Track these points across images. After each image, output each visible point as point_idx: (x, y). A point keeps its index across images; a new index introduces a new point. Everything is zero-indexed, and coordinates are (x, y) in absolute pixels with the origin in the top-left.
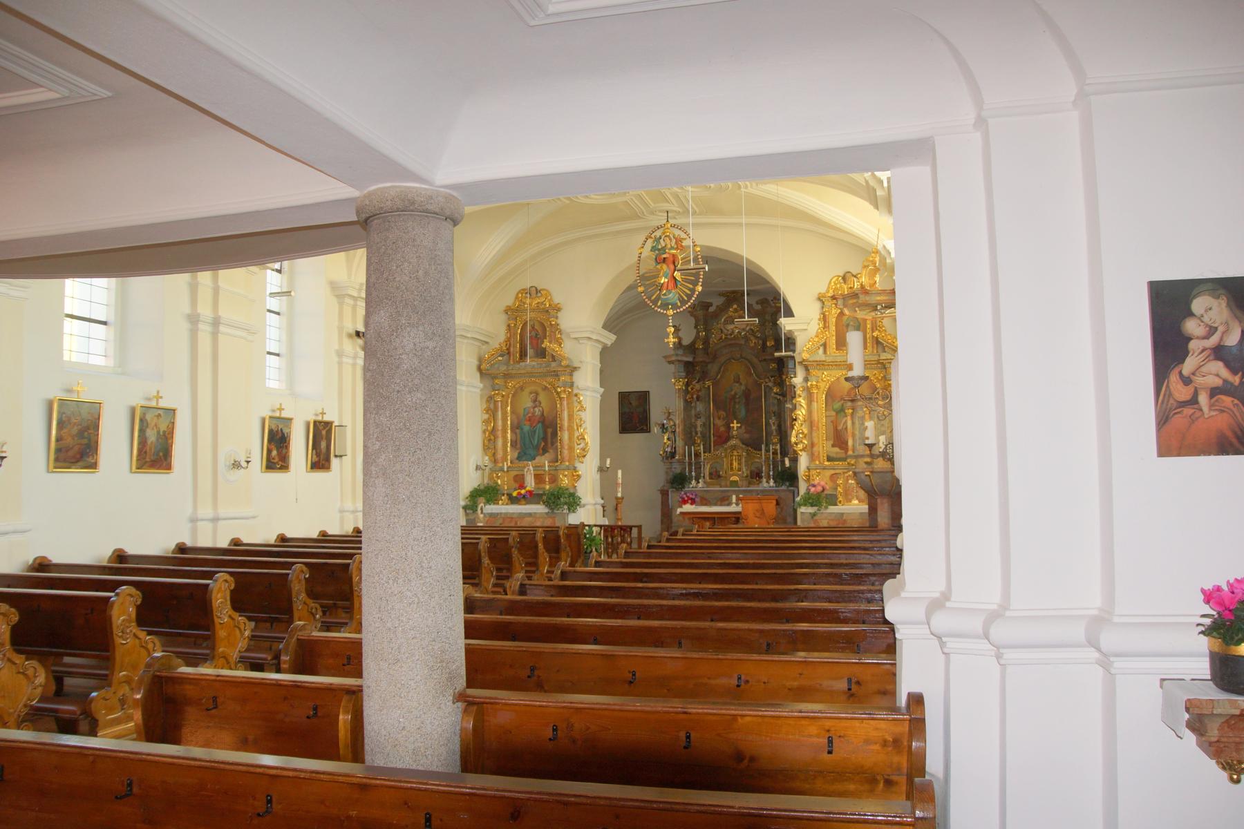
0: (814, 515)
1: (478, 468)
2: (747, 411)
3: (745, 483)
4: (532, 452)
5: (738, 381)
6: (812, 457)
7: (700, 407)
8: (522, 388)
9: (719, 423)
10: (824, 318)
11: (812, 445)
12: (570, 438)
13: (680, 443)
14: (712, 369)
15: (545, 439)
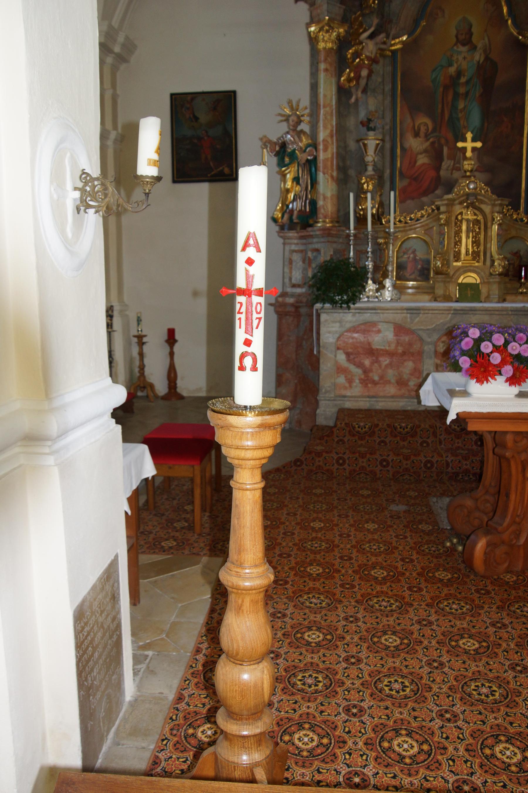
2: (486, 114)
3: (495, 290)
9: (415, 144)
13: (326, 187)
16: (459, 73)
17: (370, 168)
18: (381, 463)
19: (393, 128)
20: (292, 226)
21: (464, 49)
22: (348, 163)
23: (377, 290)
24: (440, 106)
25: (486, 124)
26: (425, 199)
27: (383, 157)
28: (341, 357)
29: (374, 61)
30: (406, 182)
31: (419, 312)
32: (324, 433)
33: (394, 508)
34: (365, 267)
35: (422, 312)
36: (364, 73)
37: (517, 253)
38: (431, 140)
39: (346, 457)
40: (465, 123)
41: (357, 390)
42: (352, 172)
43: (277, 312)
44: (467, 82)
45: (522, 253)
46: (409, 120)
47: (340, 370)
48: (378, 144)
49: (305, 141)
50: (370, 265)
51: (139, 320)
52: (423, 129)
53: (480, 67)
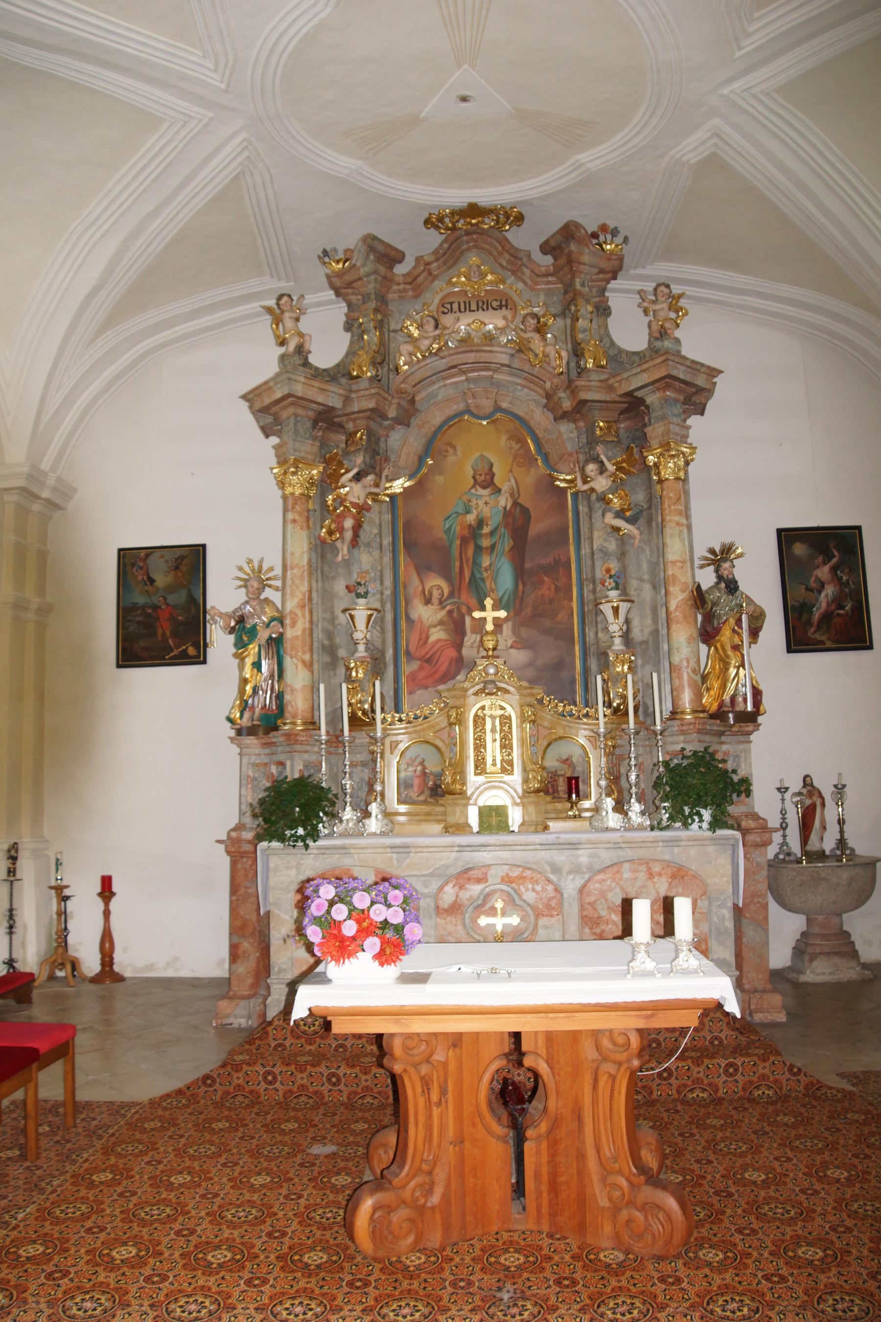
2: (520, 573)
5: (487, 481)
14: (403, 443)
16: (481, 523)
17: (361, 648)
18: (329, 1080)
20: (251, 731)
21: (486, 492)
22: (337, 640)
23: (359, 821)
24: (457, 564)
25: (521, 587)
26: (441, 687)
27: (383, 631)
30: (415, 665)
31: (407, 850)
33: (318, 1150)
34: (343, 788)
35: (413, 850)
36: (349, 523)
37: (567, 759)
38: (448, 608)
39: (276, 1070)
40: (493, 586)
42: (342, 653)
43: (228, 852)
44: (492, 533)
45: (574, 760)
46: (416, 582)
48: (371, 615)
51: (58, 864)
52: (436, 594)
53: (507, 514)
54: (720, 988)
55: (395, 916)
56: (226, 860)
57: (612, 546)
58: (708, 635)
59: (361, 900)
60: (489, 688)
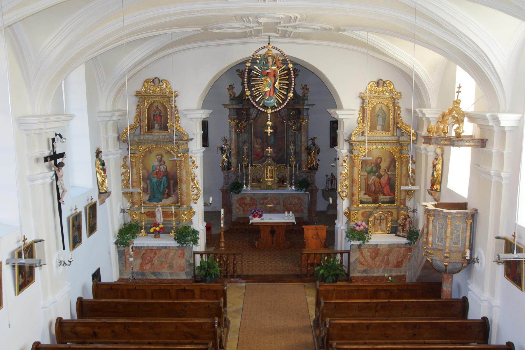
0: (359, 246)
1: (123, 211)
3: (276, 187)
4: (160, 197)
6: (352, 202)
7: (245, 136)
8: (150, 152)
9: (257, 146)
10: (363, 110)
11: (353, 195)
12: (187, 187)
13: (234, 160)
15: (168, 187)
19: (251, 142)
28: (238, 205)
29: (246, 126)
32: (234, 223)
41: (242, 212)
46: (255, 140)
47: (237, 208)
49: (228, 147)
50: (244, 181)
54: (294, 221)
55: (261, 213)
56: (221, 193)
57: (293, 134)
58: (309, 154)
59: (257, 211)
60: (270, 164)
